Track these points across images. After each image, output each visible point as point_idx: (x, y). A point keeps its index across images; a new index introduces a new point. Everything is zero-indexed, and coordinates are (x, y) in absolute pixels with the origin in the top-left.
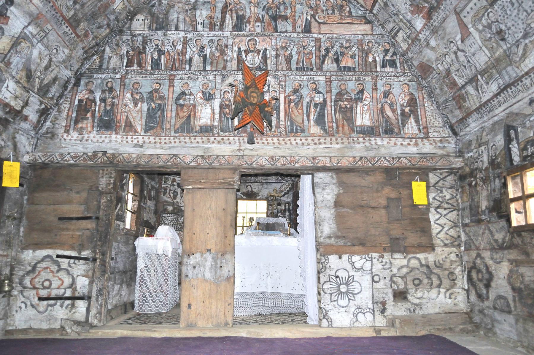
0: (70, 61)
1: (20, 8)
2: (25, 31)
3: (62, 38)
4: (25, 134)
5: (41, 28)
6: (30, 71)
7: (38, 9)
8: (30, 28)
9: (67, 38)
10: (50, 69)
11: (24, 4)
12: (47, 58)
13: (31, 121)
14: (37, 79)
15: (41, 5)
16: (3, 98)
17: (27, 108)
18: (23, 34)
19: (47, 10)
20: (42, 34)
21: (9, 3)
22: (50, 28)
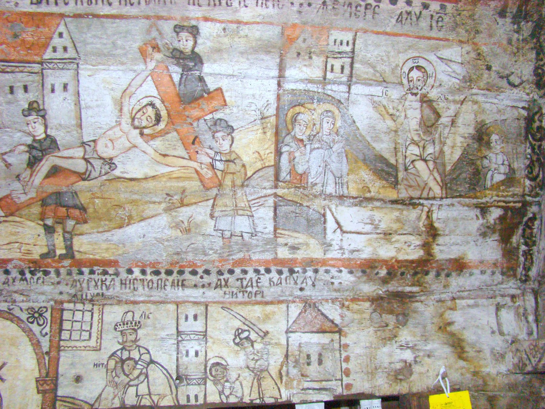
0: (489, 68)
1: (225, 56)
2: (289, 86)
3: (407, 35)
4: (484, 301)
5: (322, 52)
6: (382, 159)
7: (271, 24)
8: (290, 73)
9: (424, 24)
10: (444, 120)
11: (226, 40)
12: (413, 102)
13: (481, 262)
14: (420, 165)
15: (271, 11)
16: (346, 256)
17: (440, 240)
18: (286, 98)
19: (296, 8)
20: (337, 64)
21: (191, 64)
22: (349, 36)
